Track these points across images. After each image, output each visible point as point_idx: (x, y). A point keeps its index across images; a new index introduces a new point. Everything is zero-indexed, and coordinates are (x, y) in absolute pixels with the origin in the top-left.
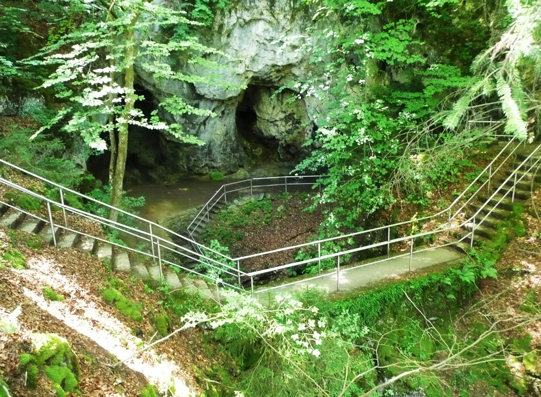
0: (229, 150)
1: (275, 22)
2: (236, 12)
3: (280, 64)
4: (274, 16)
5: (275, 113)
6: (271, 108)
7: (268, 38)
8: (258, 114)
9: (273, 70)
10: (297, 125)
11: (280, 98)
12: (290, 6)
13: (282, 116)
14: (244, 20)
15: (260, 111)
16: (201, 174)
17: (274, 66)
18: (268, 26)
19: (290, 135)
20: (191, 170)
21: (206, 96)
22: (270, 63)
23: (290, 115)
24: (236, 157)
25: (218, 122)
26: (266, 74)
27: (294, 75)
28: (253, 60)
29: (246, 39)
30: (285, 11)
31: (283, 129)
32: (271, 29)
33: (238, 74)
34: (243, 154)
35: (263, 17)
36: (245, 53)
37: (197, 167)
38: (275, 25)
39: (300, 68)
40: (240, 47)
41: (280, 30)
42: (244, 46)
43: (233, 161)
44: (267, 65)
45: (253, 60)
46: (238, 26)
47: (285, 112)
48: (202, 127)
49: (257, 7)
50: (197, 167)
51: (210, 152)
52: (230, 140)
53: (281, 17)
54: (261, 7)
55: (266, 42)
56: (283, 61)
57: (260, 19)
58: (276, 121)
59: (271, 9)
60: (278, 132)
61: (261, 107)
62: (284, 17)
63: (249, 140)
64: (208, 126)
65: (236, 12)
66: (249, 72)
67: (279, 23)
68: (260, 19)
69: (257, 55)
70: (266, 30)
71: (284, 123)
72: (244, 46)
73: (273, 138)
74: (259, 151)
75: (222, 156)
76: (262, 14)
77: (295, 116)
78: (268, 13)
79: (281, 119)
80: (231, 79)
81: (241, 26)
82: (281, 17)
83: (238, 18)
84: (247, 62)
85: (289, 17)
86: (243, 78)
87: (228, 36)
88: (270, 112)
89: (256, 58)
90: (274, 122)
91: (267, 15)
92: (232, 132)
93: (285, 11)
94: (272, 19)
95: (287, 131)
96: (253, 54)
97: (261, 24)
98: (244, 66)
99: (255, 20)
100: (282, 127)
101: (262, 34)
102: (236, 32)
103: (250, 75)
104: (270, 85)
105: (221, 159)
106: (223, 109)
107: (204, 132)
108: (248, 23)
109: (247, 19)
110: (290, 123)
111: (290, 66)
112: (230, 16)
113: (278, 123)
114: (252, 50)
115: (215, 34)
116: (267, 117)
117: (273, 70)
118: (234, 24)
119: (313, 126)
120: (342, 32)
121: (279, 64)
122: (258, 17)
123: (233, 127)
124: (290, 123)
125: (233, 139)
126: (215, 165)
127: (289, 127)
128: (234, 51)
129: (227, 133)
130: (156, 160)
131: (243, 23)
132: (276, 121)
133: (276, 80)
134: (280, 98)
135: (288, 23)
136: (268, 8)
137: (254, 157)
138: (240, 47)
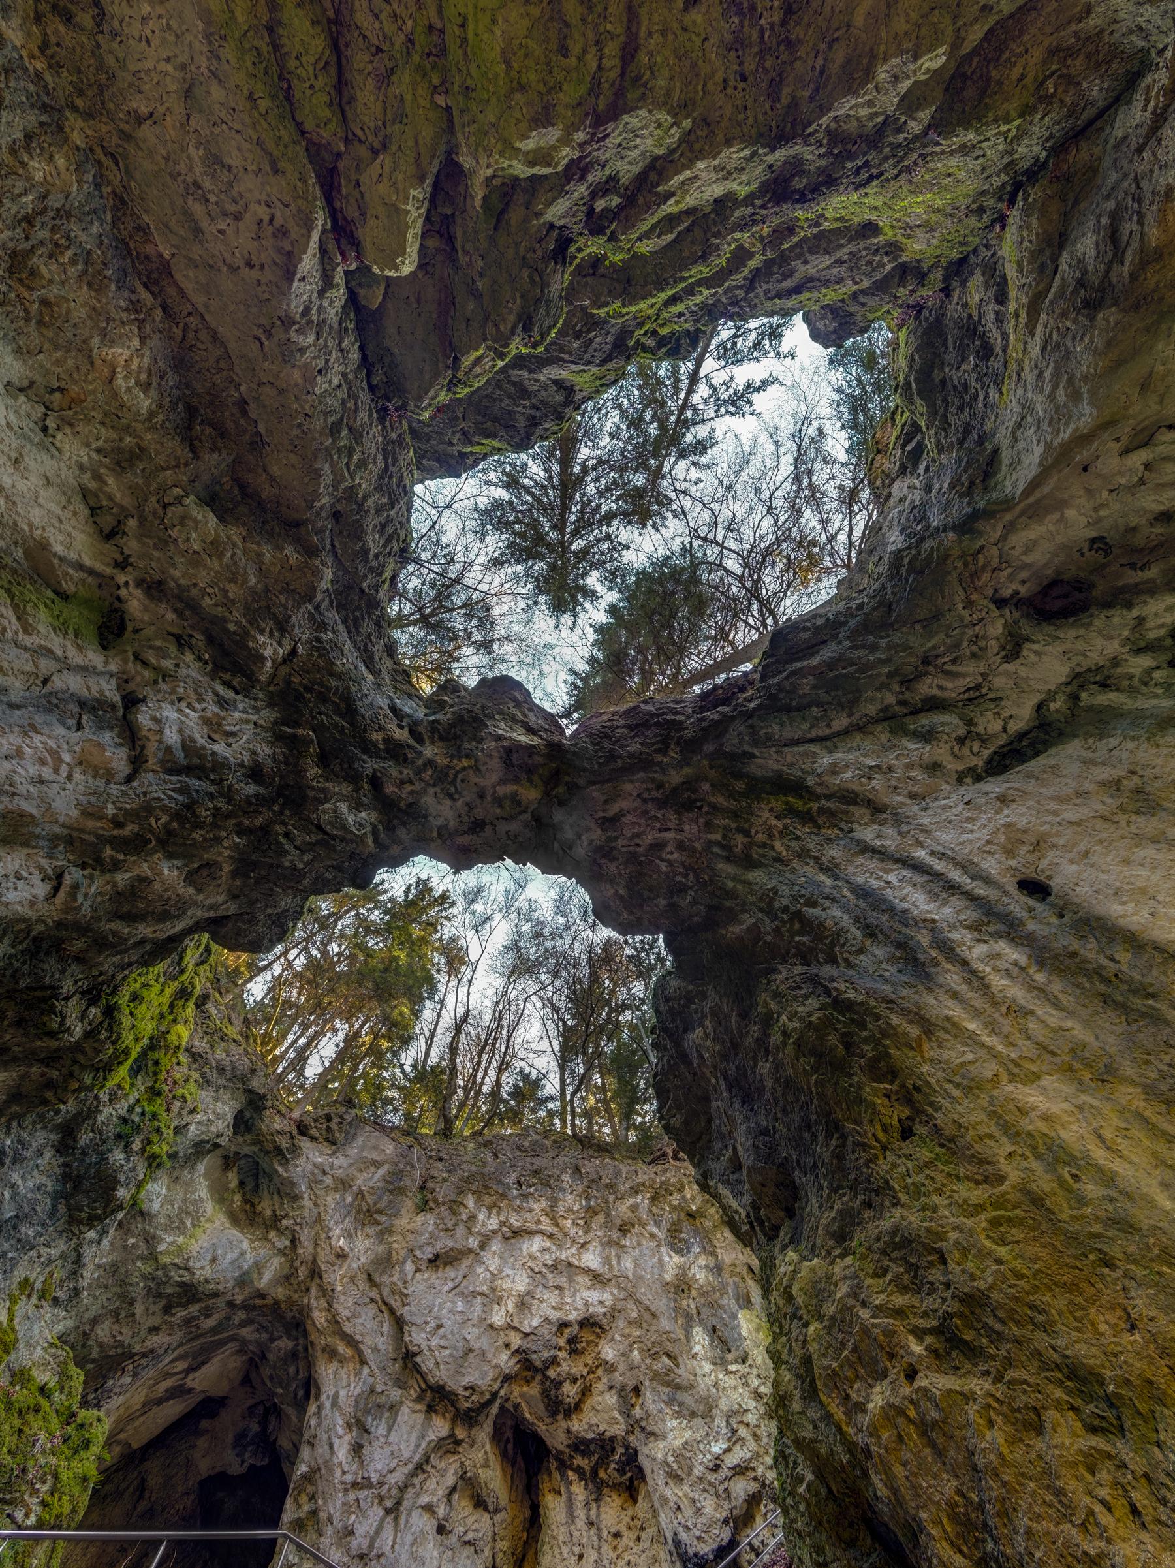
1: (560, 1235)
2: (498, 1214)
3: (573, 1316)
4: (557, 1225)
7: (549, 1263)
11: (593, 1512)
18: (548, 1243)
21: (418, 1359)
22: (554, 1315)
28: (523, 1304)
32: (554, 1249)
33: (491, 1326)
36: (506, 1284)
39: (613, 1339)
40: (501, 1271)
44: (547, 1320)
46: (499, 1236)
53: (568, 1223)
56: (576, 1309)
65: (498, 1214)
66: (512, 1333)
67: (566, 1235)
69: (528, 1293)
70: (545, 1250)
72: (507, 1271)
76: (539, 1222)
80: (476, 1331)
81: (505, 1238)
82: (568, 1223)
83: (502, 1224)
84: (511, 1306)
85: (581, 1222)
86: (501, 1342)
94: (555, 1230)
98: (503, 1312)
99: (531, 1233)
102: (496, 1246)
103: (516, 1341)
108: (517, 1233)
114: (521, 1283)
118: (494, 1232)
131: (509, 1234)
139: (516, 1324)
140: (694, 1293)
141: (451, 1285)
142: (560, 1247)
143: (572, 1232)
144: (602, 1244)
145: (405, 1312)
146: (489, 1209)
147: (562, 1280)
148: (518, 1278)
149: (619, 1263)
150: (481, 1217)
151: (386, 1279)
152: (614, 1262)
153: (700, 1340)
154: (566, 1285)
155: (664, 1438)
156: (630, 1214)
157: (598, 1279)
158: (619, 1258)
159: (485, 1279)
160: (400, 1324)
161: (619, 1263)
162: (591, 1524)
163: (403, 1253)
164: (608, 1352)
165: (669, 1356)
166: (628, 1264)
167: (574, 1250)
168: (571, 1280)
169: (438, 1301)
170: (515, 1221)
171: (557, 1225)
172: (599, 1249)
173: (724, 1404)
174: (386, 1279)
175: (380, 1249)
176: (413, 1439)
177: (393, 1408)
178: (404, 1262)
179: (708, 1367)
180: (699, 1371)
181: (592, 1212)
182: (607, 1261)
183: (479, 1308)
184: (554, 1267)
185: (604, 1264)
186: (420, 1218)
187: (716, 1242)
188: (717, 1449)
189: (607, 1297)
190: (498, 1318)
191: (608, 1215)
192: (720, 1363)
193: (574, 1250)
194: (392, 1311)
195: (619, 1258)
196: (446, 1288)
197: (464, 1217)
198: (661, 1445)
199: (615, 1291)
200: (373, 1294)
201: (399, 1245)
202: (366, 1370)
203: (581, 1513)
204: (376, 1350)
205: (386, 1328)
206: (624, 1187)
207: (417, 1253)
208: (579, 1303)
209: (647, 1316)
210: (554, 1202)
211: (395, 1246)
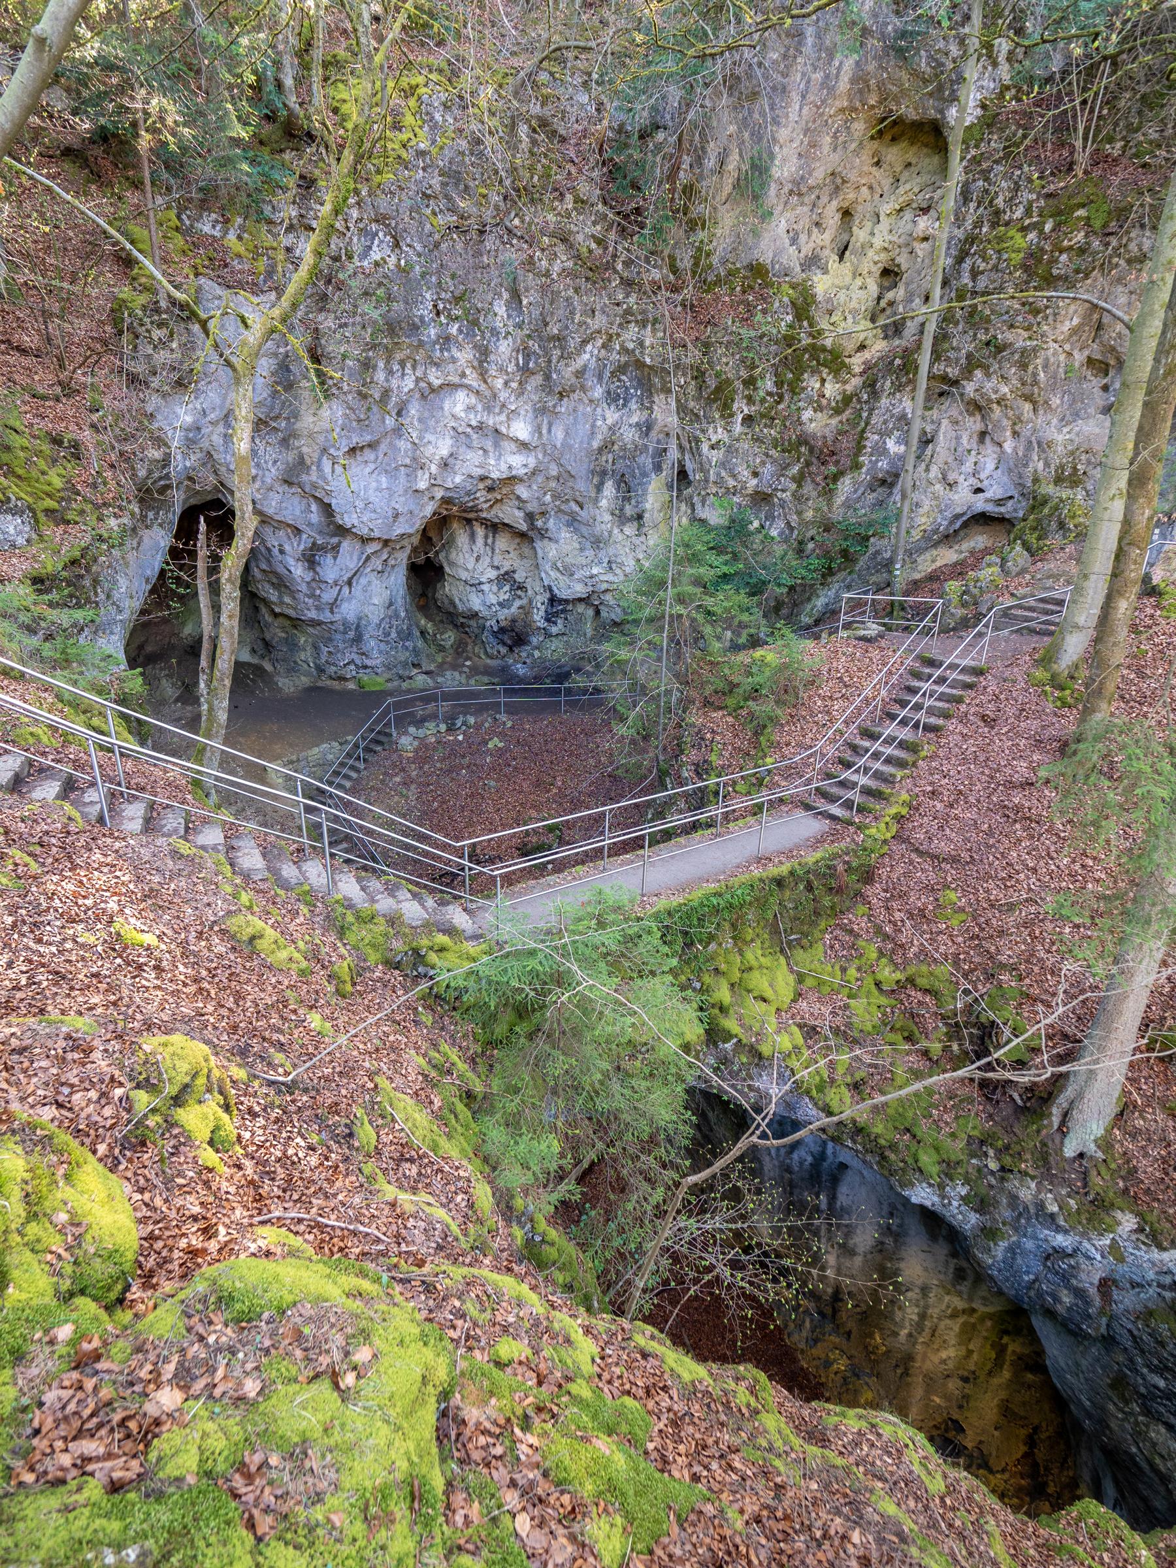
0: (394, 635)
1: (488, 393)
2: (414, 368)
3: (495, 475)
4: (485, 382)
5: (480, 567)
6: (472, 560)
7: (474, 423)
8: (447, 569)
9: (481, 486)
10: (519, 592)
11: (490, 541)
12: (517, 365)
13: (492, 574)
14: (429, 384)
15: (452, 564)
16: (342, 679)
17: (483, 478)
18: (473, 400)
19: (506, 611)
20: (323, 671)
22: (478, 472)
23: (507, 573)
24: (407, 648)
25: (376, 582)
26: (468, 493)
27: (518, 498)
28: (446, 465)
29: (432, 423)
30: (507, 373)
31: (493, 599)
32: (479, 407)
34: (420, 643)
35: (466, 381)
36: (429, 451)
37: (334, 664)
38: (490, 401)
40: (421, 438)
41: (497, 410)
42: (429, 437)
43: (403, 656)
45: (446, 465)
47: (498, 568)
48: (346, 590)
49: (454, 360)
50: (334, 664)
51: (358, 639)
52: (397, 616)
53: (499, 383)
54: (462, 362)
55: (469, 430)
57: (461, 386)
58: (481, 583)
59: (481, 366)
60: (484, 603)
61: (453, 556)
62: (506, 383)
63: (429, 618)
64: (357, 589)
65: (414, 368)
67: (495, 396)
68: (461, 386)
71: (495, 588)
73: (475, 615)
74: (449, 637)
75: (383, 646)
76: (463, 375)
77: (516, 576)
78: (475, 375)
79: (490, 581)
83: (418, 380)
84: (434, 469)
85: (514, 385)
87: (399, 414)
88: (470, 566)
89: (451, 461)
90: (477, 585)
91: (472, 379)
92: (400, 601)
93: (507, 373)
94: (483, 387)
95: (500, 604)
96: (445, 452)
97: (461, 395)
98: (427, 476)
99: (453, 387)
100: (491, 596)
101: (463, 415)
102: (414, 410)
103: (439, 494)
104: (472, 515)
105: (380, 652)
106: (385, 556)
107: (349, 600)
109: (437, 382)
110: (507, 588)
111: (512, 480)
112: (403, 375)
113: (485, 587)
114: (443, 447)
115: (375, 409)
116: (464, 575)
117: (481, 486)
119: (548, 595)
120: (609, 421)
121: (493, 476)
122: (455, 379)
123: (401, 592)
124: (507, 588)
125: (403, 614)
126: (368, 662)
127: (504, 596)
128: (409, 446)
129: (391, 604)
130: (253, 651)
132: (481, 583)
133: (485, 506)
134: (490, 541)
135: (513, 398)
136: (476, 364)
137: (441, 649)
138: (421, 438)
139: (439, 482)
140: (616, 447)
141: (372, 466)
142: (488, 409)
143: (503, 395)
144: (535, 410)
145: (334, 502)
146: (402, 364)
147: (489, 445)
148: (440, 443)
149: (549, 431)
150: (394, 383)
151: (304, 478)
152: (544, 431)
153: (609, 489)
154: (490, 449)
155: (557, 542)
156: (574, 380)
157: (524, 446)
158: (550, 425)
159: (406, 452)
160: (327, 509)
161: (549, 431)
162: (486, 544)
163: (316, 455)
164: (522, 491)
165: (577, 502)
166: (559, 434)
167: (503, 417)
168: (496, 445)
169: (362, 484)
170: (435, 378)
171: (485, 382)
172: (530, 415)
173: (611, 551)
174: (304, 478)
175: (291, 457)
176: (355, 558)
177: (336, 549)
178: (320, 460)
179: (607, 517)
180: (599, 518)
181: (525, 371)
182: (538, 430)
183: (402, 479)
184: (480, 428)
185: (532, 434)
186: (325, 413)
187: (656, 399)
188: (595, 571)
189: (532, 462)
190: (422, 485)
191: (547, 377)
192: (621, 518)
193: (503, 417)
194: (315, 497)
195: (550, 425)
196: (368, 470)
197: (377, 396)
198: (553, 546)
199: (540, 456)
200: (293, 490)
201: (309, 450)
202: (304, 536)
203: (480, 541)
204: (310, 524)
205: (314, 507)
206: (572, 344)
207: (332, 451)
208: (504, 467)
209: (565, 475)
210: (484, 353)
211: (305, 450)
